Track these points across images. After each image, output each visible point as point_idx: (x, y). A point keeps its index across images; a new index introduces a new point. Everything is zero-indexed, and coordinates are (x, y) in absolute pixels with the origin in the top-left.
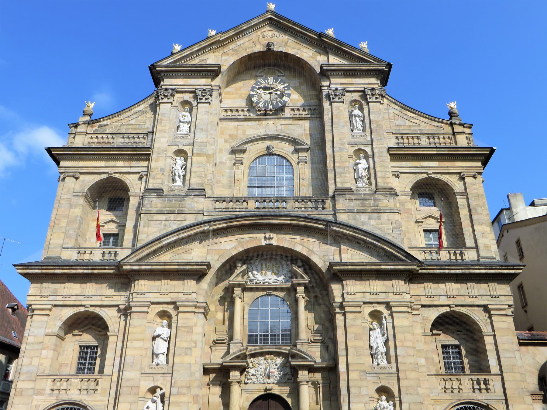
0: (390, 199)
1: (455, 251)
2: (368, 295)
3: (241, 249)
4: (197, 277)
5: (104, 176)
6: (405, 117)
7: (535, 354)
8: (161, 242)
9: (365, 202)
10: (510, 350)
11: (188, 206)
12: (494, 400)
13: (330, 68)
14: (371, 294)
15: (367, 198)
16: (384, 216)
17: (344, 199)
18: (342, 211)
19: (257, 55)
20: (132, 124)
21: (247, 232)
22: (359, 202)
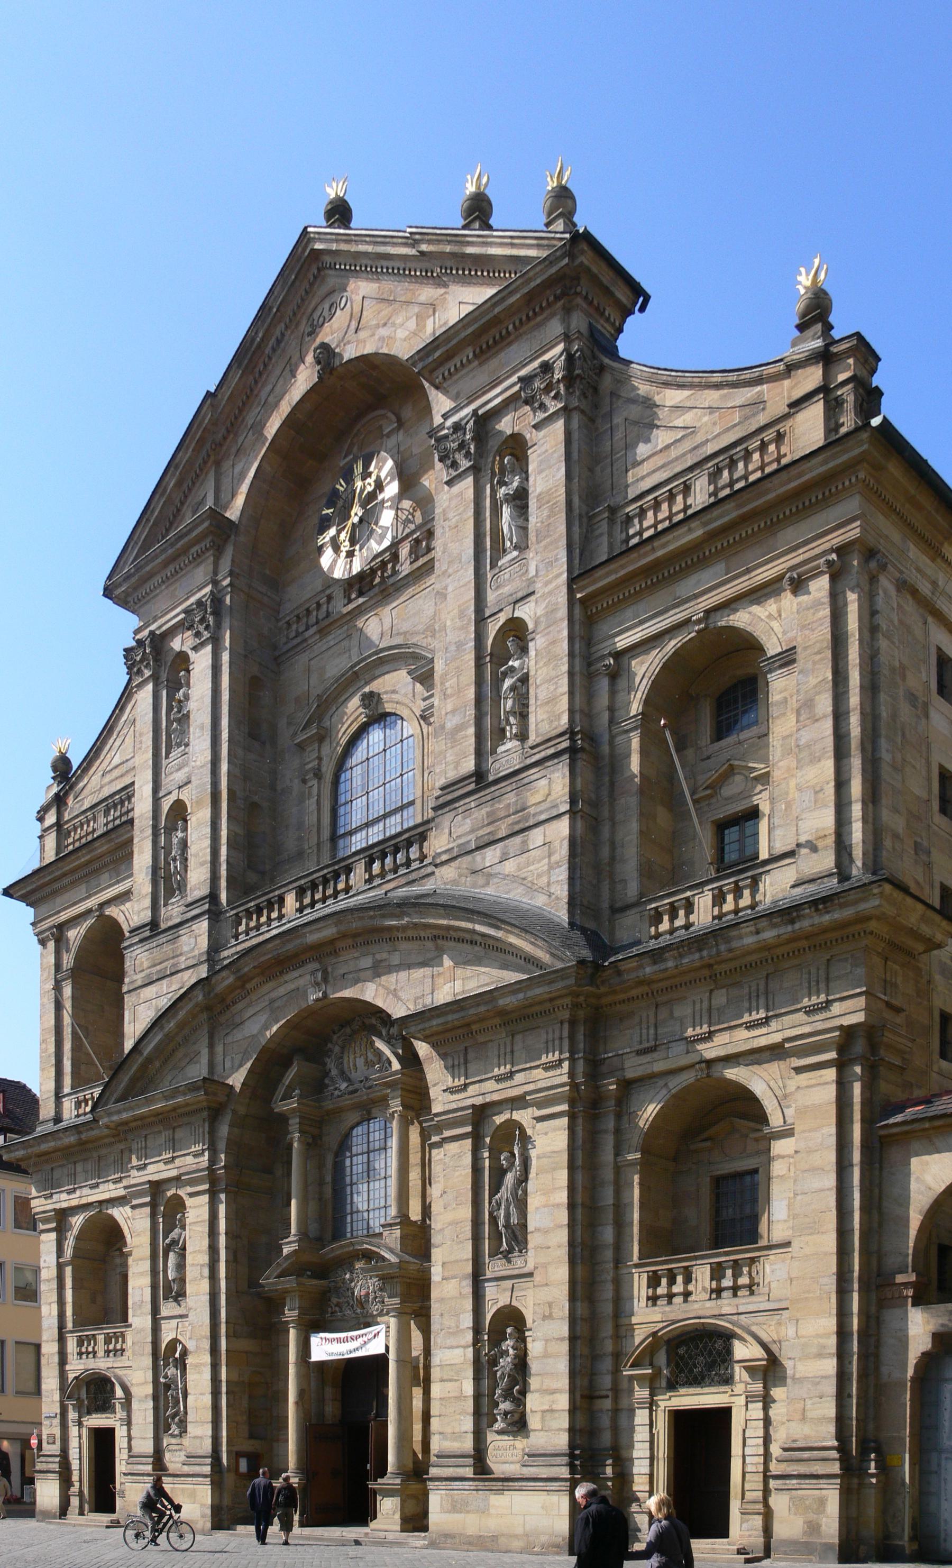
0: (553, 772)
9: (497, 806)
15: (503, 791)
16: (537, 837)
22: (484, 811)
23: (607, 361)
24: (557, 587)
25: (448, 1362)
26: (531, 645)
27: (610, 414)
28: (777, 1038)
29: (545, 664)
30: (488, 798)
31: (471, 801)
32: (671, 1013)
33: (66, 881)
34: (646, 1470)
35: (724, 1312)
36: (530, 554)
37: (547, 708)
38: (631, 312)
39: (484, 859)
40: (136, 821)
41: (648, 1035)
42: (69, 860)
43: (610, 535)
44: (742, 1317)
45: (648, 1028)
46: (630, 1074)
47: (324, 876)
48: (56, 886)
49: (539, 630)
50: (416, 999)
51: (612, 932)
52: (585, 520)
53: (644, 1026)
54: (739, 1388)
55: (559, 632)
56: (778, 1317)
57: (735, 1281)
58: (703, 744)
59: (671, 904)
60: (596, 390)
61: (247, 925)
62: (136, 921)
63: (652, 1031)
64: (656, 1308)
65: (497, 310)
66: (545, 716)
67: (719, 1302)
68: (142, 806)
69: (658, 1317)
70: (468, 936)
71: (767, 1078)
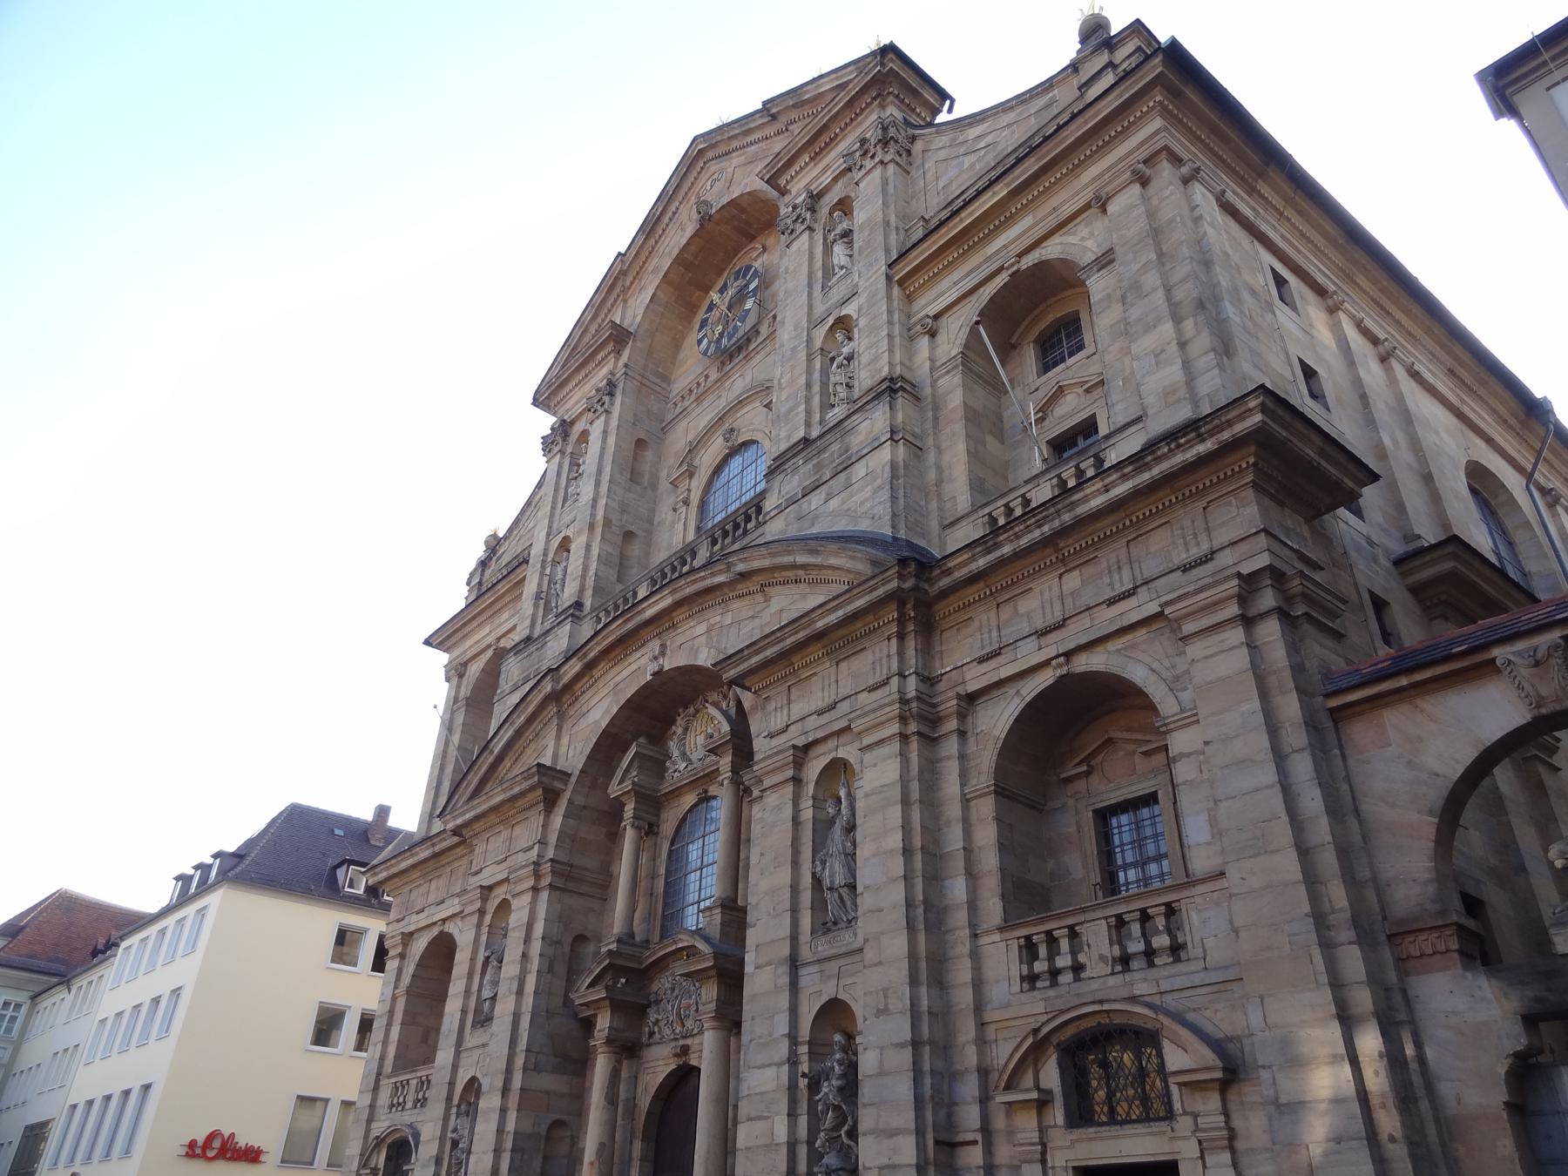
1: (1077, 467)
2: (813, 722)
3: (615, 710)
5: (490, 653)
7: (1420, 739)
10: (1252, 761)
12: (1198, 991)
14: (820, 713)
15: (827, 443)
16: (860, 470)
17: (782, 475)
19: (693, 248)
21: (627, 663)
22: (810, 466)
30: (814, 452)
35: (1138, 992)
37: (869, 368)
41: (990, 638)
44: (1168, 998)
45: (990, 631)
46: (972, 687)
53: (985, 630)
54: (1184, 1124)
55: (880, 308)
57: (1148, 943)
63: (995, 634)
67: (1128, 977)
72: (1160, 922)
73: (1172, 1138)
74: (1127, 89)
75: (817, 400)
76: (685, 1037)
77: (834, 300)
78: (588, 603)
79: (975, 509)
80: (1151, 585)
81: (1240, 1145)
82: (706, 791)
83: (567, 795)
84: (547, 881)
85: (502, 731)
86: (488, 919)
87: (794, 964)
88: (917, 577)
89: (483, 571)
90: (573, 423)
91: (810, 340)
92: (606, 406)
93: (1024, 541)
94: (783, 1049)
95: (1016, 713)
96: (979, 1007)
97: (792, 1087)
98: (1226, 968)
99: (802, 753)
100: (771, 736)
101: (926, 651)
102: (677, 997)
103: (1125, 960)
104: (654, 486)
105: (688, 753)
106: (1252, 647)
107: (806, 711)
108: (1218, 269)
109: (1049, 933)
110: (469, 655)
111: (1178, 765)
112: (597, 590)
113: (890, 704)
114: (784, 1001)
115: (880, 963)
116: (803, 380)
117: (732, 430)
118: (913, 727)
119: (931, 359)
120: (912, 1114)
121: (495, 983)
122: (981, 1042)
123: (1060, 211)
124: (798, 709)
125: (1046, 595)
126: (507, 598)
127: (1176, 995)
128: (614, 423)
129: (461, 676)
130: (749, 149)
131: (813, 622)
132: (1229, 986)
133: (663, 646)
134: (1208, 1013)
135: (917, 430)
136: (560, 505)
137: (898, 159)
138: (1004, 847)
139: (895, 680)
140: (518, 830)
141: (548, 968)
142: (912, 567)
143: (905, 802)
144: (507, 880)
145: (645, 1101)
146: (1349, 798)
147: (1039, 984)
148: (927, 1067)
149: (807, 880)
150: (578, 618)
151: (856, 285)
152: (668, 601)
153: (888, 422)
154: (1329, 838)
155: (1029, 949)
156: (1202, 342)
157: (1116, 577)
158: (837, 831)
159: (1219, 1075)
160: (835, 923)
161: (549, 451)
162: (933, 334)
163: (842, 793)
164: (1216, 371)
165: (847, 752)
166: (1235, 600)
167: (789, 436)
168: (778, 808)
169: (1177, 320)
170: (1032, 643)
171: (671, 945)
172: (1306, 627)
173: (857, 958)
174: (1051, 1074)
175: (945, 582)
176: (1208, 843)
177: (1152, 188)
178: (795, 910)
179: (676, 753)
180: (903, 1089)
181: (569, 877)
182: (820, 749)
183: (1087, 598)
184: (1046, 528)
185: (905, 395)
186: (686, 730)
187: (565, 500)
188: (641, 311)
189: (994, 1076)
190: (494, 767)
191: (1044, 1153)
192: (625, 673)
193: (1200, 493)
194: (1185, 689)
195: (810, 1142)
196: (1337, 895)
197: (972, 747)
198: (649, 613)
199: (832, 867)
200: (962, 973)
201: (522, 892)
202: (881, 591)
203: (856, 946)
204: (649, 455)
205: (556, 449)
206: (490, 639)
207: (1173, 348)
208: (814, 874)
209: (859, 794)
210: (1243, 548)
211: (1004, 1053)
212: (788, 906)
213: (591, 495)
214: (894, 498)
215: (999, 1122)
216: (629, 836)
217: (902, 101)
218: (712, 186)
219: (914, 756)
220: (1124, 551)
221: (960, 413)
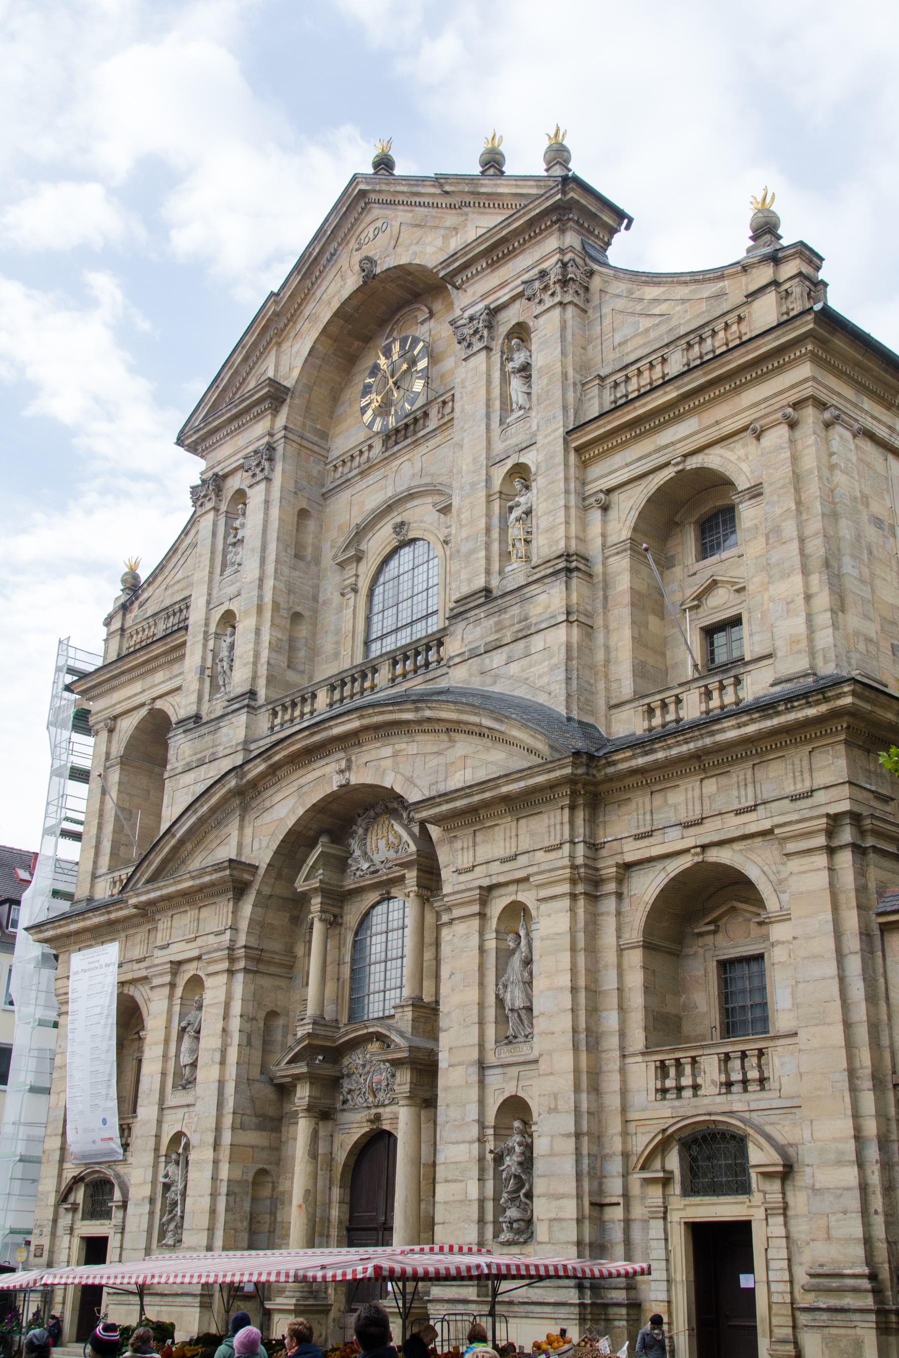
0: (552, 587)
1: (721, 682)
2: (496, 867)
3: (301, 811)
4: (230, 895)
5: (143, 712)
6: (638, 308)
8: (174, 836)
9: (503, 616)
11: (224, 739)
13: (451, 268)
14: (503, 861)
15: (508, 604)
16: (537, 643)
17: (464, 623)
18: (457, 660)
19: (354, 302)
20: (178, 582)
21: (311, 768)
22: (492, 621)
23: (596, 267)
24: (555, 439)
25: (453, 1160)
26: (534, 484)
27: (600, 306)
28: (766, 825)
29: (545, 500)
30: (496, 609)
31: (481, 613)
32: (666, 801)
33: (123, 679)
34: (663, 1296)
35: (735, 1109)
36: (533, 414)
38: (616, 231)
39: (492, 661)
40: (190, 628)
42: (127, 660)
43: (600, 396)
44: (754, 1114)
45: (644, 814)
46: (629, 858)
47: (352, 676)
48: (115, 683)
49: (540, 472)
50: (431, 785)
51: (608, 726)
52: (579, 386)
53: (641, 812)
54: (757, 1198)
56: (790, 1116)
57: (745, 1074)
58: (690, 562)
59: (663, 700)
60: (587, 289)
61: (283, 718)
62: (183, 714)
63: (648, 817)
64: (665, 1102)
65: (504, 233)
66: (545, 542)
67: (729, 1097)
68: (196, 616)
69: (667, 1113)
70: (476, 729)
71: (761, 863)
72: (754, 1061)
73: (749, 1207)
74: (784, 334)
75: (495, 547)
76: (377, 1106)
77: (513, 441)
78: (262, 693)
79: (638, 696)
80: (768, 806)
81: (790, 1213)
82: (388, 893)
83: (256, 886)
84: (242, 964)
85: (185, 818)
86: (179, 992)
87: (482, 1066)
88: (588, 766)
89: (124, 615)
90: (225, 477)
91: (488, 480)
92: (266, 472)
93: (674, 752)
94: (474, 1131)
95: (662, 885)
96: (624, 1110)
97: (481, 1159)
98: (793, 1097)
99: (487, 892)
100: (459, 872)
101: (592, 821)
102: (368, 1072)
103: (729, 1084)
104: (317, 560)
105: (370, 854)
106: (831, 869)
107: (489, 857)
108: (843, 523)
109: (677, 1060)
110: (118, 710)
111: (775, 949)
112: (270, 679)
113: (563, 868)
114: (474, 1094)
115: (552, 1074)
116: (482, 523)
117: (402, 524)
118: (580, 888)
119: (604, 536)
120: (574, 1184)
121: (194, 1051)
122: (625, 1134)
123: (722, 425)
124: (485, 851)
125: (690, 794)
126: (162, 660)
127: (759, 1113)
128: (276, 494)
129: (111, 731)
130: (418, 209)
131: (498, 786)
132: (794, 1110)
133: (349, 761)
134: (779, 1127)
135: (589, 608)
136: (218, 570)
137: (576, 300)
138: (648, 990)
139: (566, 847)
140: (205, 913)
141: (247, 1042)
142: (584, 759)
143: (573, 950)
144: (199, 958)
145: (341, 1156)
146: (883, 988)
147: (668, 1096)
148: (585, 1151)
149: (491, 999)
150: (254, 708)
151: (534, 435)
152: (355, 724)
153: (564, 603)
154: (865, 1018)
155: (662, 1068)
156: (823, 600)
157: (743, 792)
158: (516, 961)
159: (780, 1169)
160: (515, 1037)
161: (201, 505)
162: (605, 509)
163: (522, 933)
164: (830, 630)
165: (527, 897)
166: (823, 833)
167: (470, 581)
168: (467, 936)
169: (806, 572)
170: (675, 833)
171: (362, 1029)
172: (871, 856)
173: (533, 1066)
174: (673, 1161)
175: (611, 770)
176: (790, 1010)
177: (799, 433)
178: (481, 1023)
179: (357, 853)
180: (568, 1166)
181: (259, 960)
182: (502, 891)
183: (721, 804)
184: (692, 746)
185: (580, 575)
186: (367, 830)
187: (224, 566)
188: (299, 363)
189: (634, 1159)
190: (176, 849)
191: (665, 1213)
192: (310, 777)
193: (807, 741)
194: (784, 892)
195: (496, 1199)
196: (865, 1057)
197: (626, 907)
198: (336, 731)
199: (512, 992)
200: (612, 1083)
201: (216, 973)
202: (557, 774)
203: (532, 1057)
204: (311, 525)
205: (209, 505)
206: (145, 697)
207: (800, 601)
208: (497, 996)
209: (534, 935)
210: (833, 792)
211: (641, 1142)
212: (476, 1020)
213: (257, 574)
214: (568, 679)
215: (636, 1189)
216: (318, 927)
217: (582, 226)
218: (375, 236)
219: (581, 912)
220: (750, 772)
221: (627, 599)
